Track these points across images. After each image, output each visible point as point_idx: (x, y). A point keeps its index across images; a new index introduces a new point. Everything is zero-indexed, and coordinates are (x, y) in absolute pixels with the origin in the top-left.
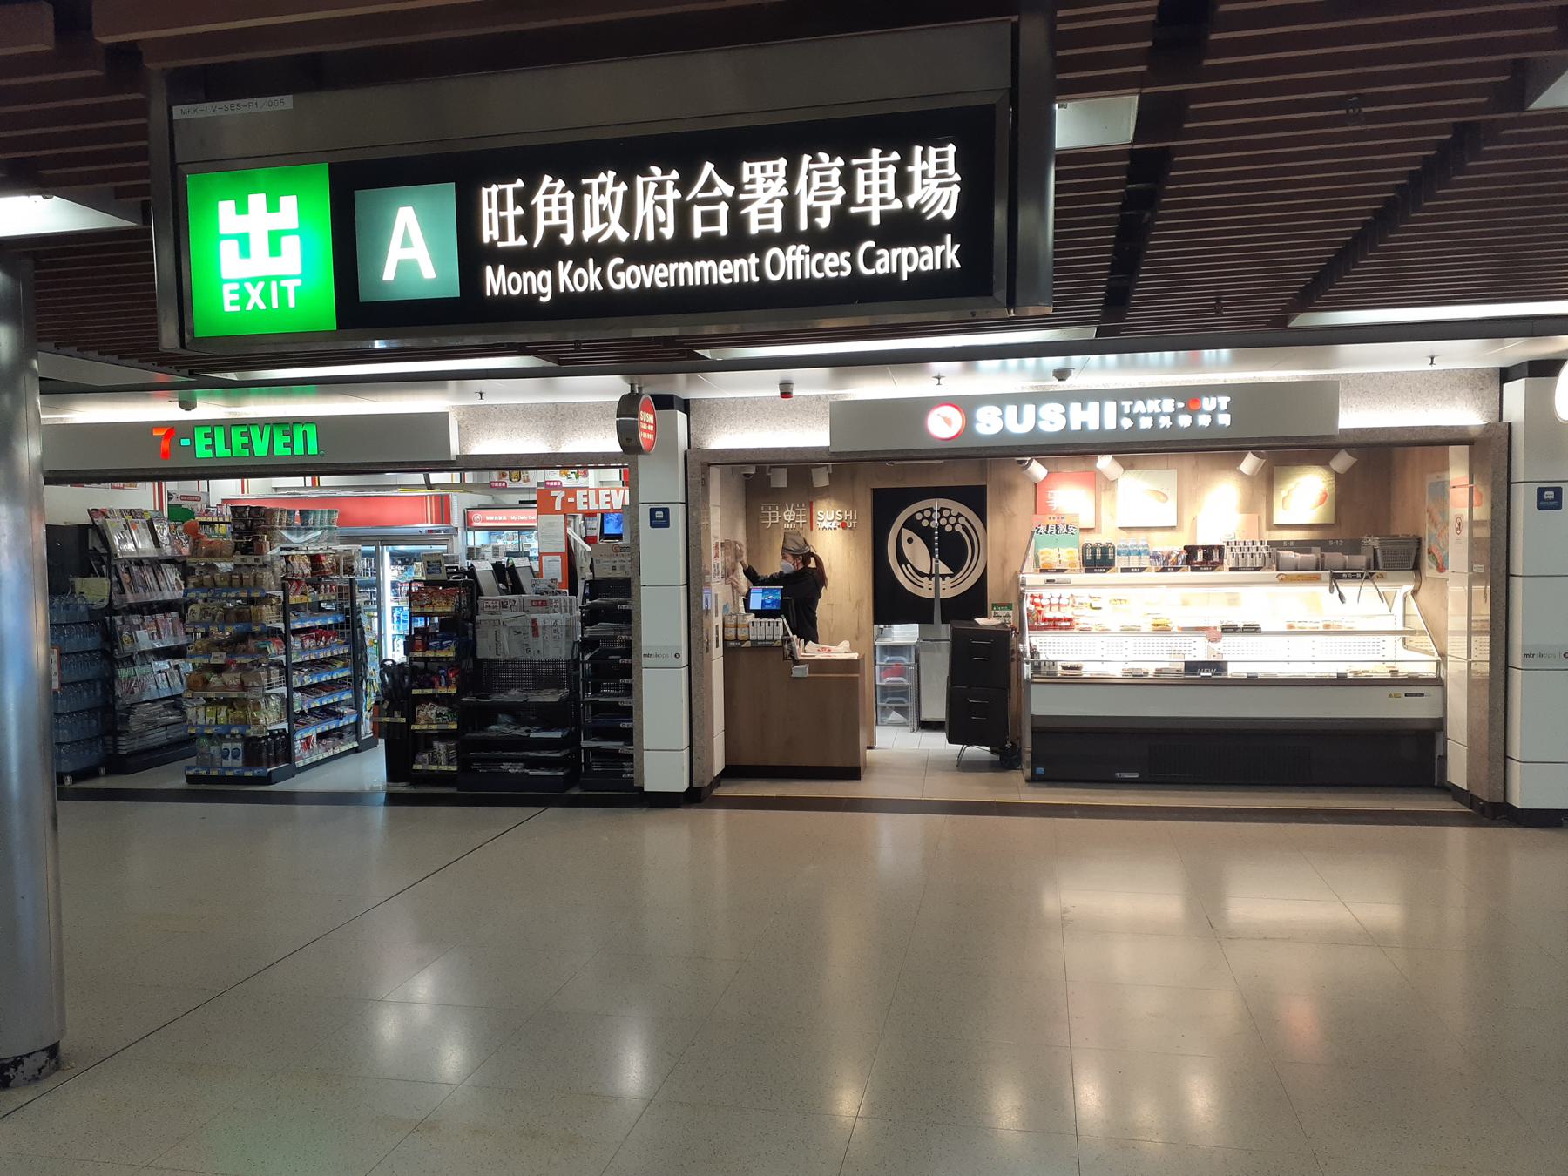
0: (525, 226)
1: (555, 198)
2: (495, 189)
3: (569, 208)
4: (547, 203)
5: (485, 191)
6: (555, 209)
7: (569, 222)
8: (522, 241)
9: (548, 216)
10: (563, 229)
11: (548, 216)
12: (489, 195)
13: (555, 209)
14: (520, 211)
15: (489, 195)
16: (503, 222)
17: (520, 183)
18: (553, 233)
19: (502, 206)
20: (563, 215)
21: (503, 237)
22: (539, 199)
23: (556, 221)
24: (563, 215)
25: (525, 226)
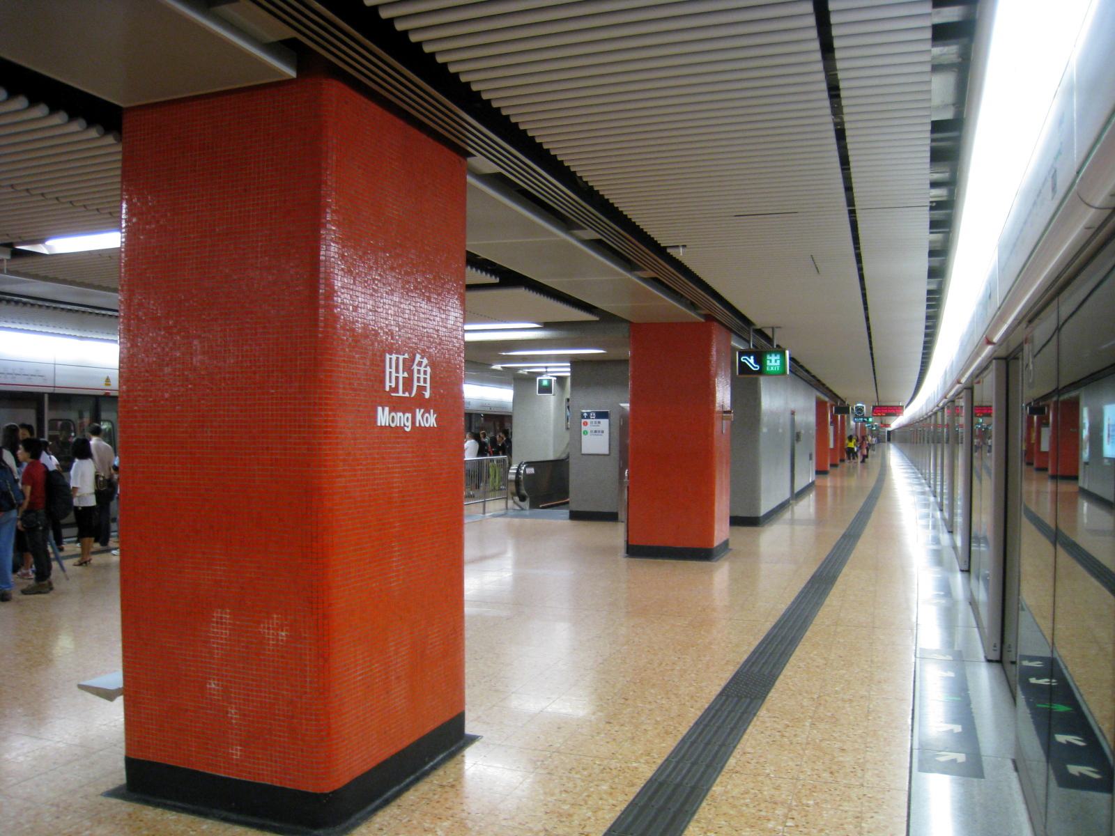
0: (408, 383)
2: (394, 357)
3: (428, 377)
4: (419, 371)
7: (428, 385)
8: (407, 395)
9: (419, 379)
12: (391, 359)
13: (422, 376)
14: (406, 375)
15: (391, 359)
16: (397, 378)
18: (421, 389)
19: (397, 371)
21: (396, 390)
23: (422, 384)
25: (408, 383)
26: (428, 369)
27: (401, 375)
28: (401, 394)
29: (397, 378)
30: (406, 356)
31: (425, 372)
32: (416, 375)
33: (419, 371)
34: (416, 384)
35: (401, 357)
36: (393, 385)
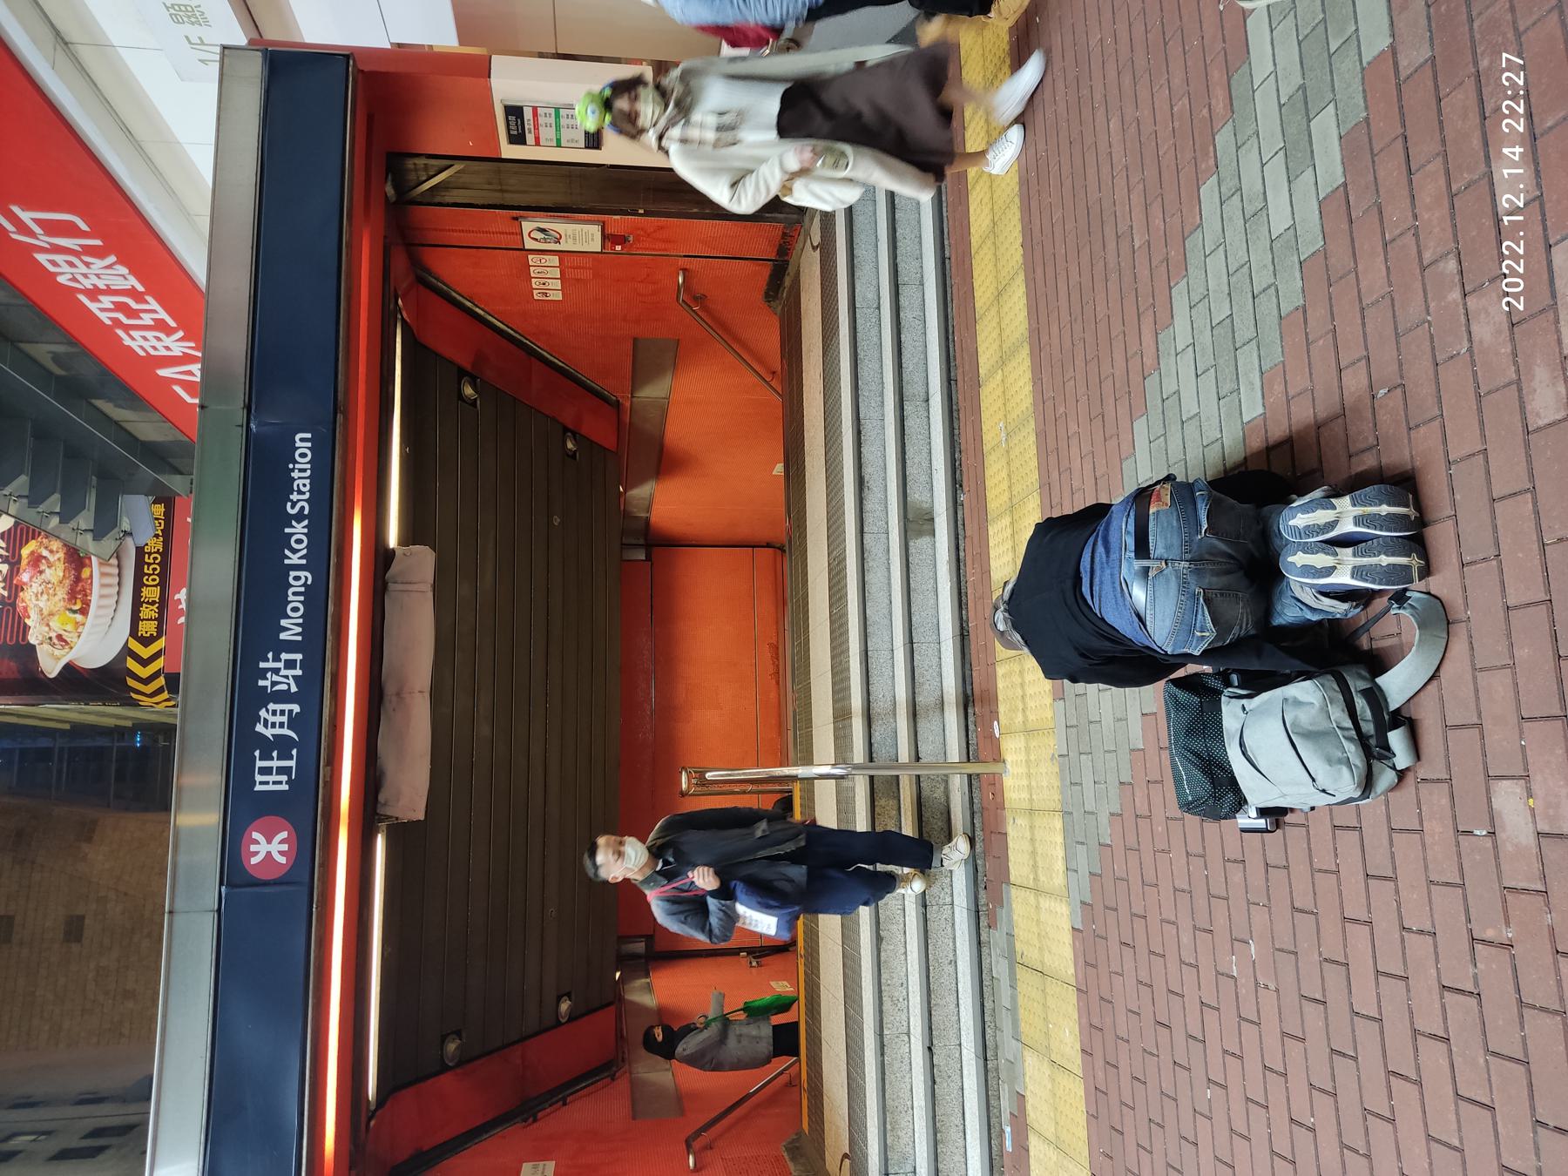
1: (271, 719)
2: (258, 778)
3: (279, 707)
4: (274, 725)
5: (258, 788)
6: (278, 719)
7: (286, 707)
8: (294, 752)
9: (282, 725)
10: (291, 711)
11: (282, 725)
13: (278, 719)
14: (275, 754)
16: (281, 771)
17: (257, 753)
20: (282, 713)
22: (269, 733)
23: (285, 719)
24: (282, 713)
26: (271, 706)
27: (275, 764)
28: (292, 763)
29: (281, 771)
30: (257, 753)
31: (274, 712)
32: (278, 731)
33: (274, 725)
34: (286, 732)
35: (259, 764)
36: (284, 778)
